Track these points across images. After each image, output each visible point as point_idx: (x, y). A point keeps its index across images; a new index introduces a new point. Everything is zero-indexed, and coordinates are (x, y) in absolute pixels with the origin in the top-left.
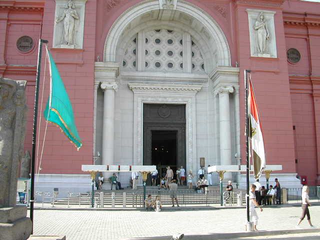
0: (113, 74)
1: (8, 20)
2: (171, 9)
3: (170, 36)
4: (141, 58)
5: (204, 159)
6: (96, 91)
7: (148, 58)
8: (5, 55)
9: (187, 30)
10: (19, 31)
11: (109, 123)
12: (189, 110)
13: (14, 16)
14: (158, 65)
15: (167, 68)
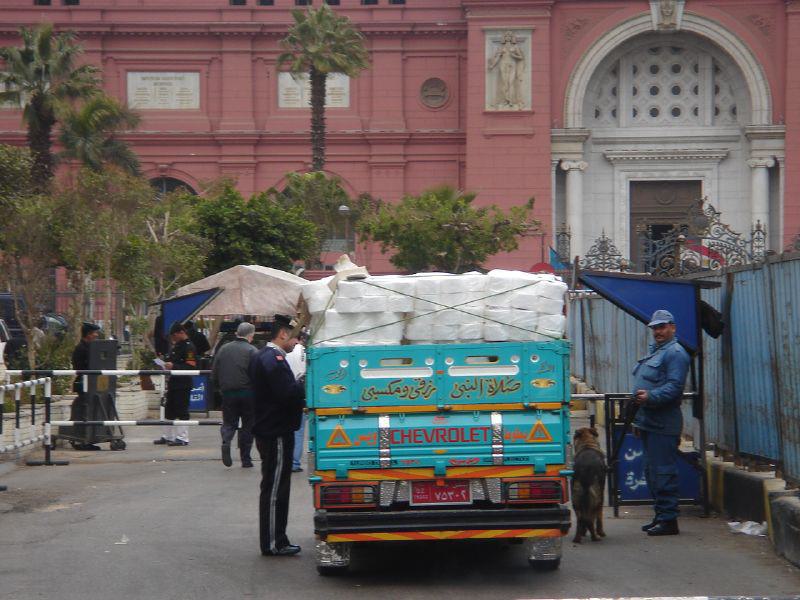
3: (675, 59)
4: (625, 101)
10: (423, 69)
13: (411, 46)
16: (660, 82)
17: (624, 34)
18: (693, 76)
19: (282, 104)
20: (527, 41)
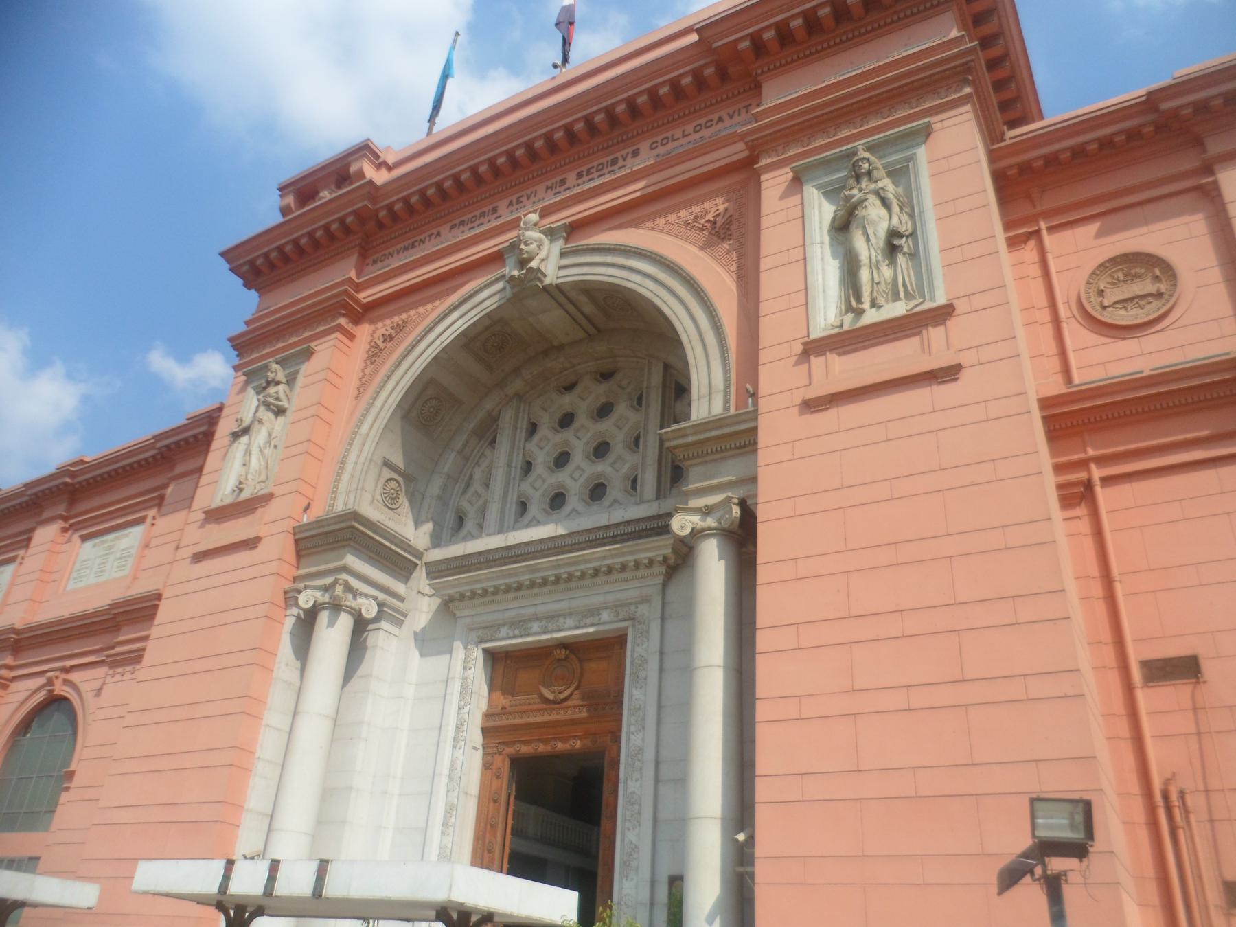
7: (526, 487)
12: (633, 652)
15: (580, 507)
16: (573, 440)
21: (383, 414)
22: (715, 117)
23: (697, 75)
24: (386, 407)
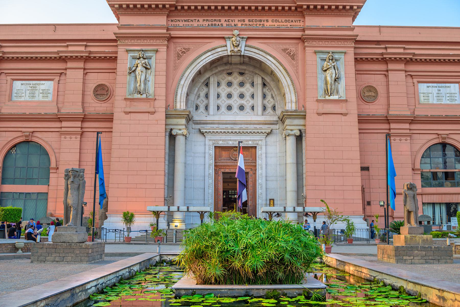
0: (183, 121)
1: (84, 69)
2: (239, 54)
3: (240, 78)
5: (273, 200)
6: (167, 137)
7: (219, 102)
8: (83, 103)
9: (257, 72)
11: (179, 167)
12: (259, 152)
13: (90, 65)
14: (229, 108)
16: (233, 92)
17: (211, 57)
18: (250, 88)
19: (14, 99)
20: (152, 58)
21: (188, 79)
22: (291, 19)
23: (290, 8)
24: (188, 77)
